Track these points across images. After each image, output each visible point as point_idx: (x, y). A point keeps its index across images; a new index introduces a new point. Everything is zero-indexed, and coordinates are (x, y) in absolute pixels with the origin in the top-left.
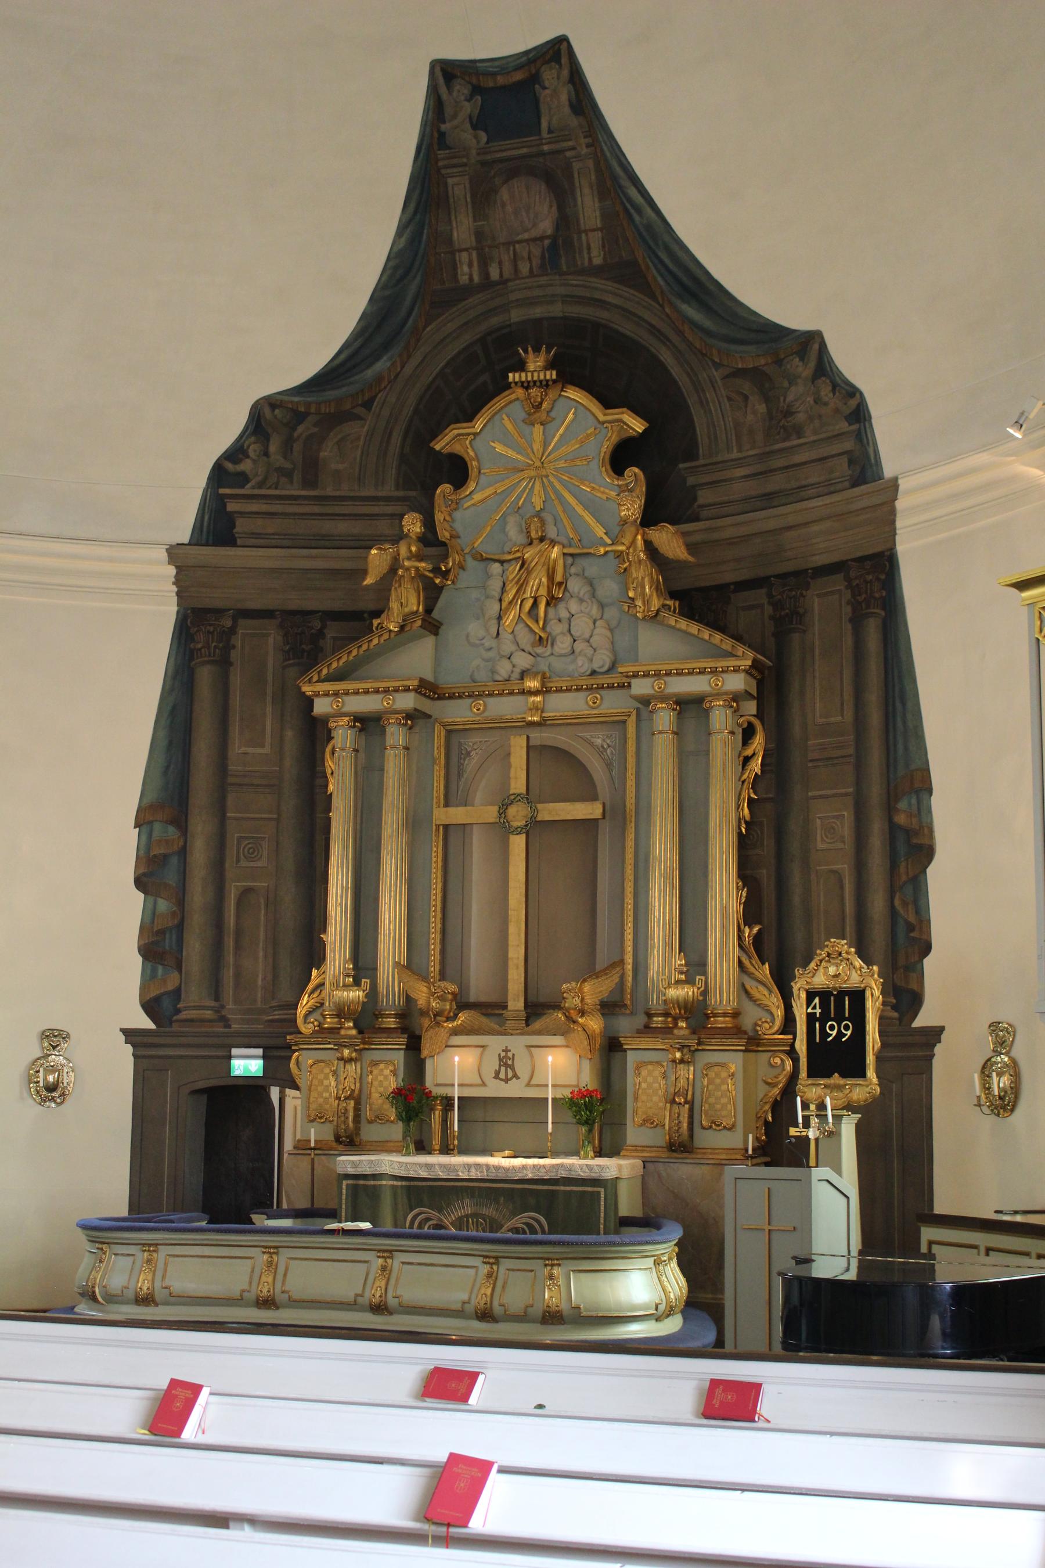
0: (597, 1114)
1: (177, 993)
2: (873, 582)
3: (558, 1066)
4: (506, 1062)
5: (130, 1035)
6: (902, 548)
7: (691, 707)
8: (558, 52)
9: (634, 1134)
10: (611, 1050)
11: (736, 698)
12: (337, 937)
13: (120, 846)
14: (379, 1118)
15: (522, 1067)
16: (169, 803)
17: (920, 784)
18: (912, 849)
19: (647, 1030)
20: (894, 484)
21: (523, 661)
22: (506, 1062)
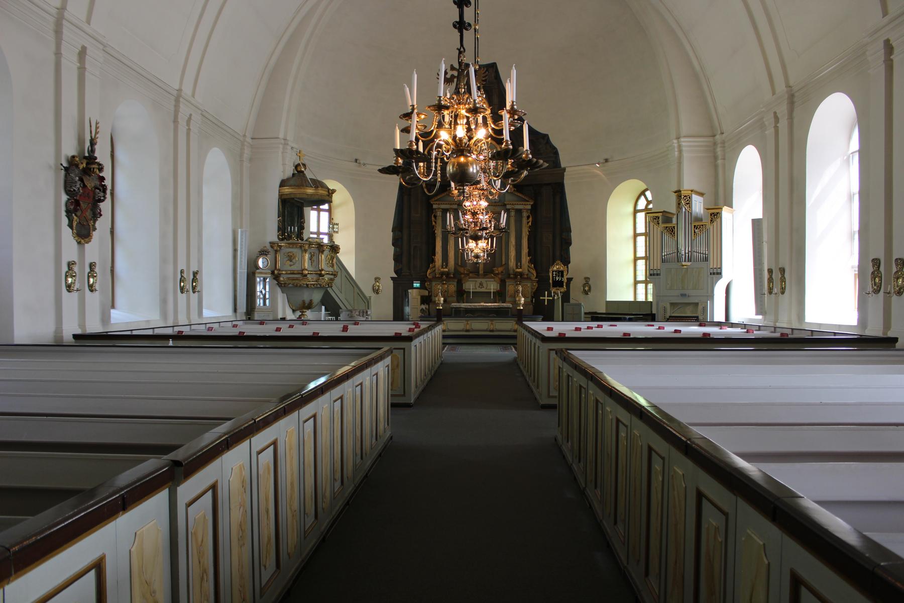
0: (500, 295)
1: (401, 269)
2: (558, 189)
3: (492, 286)
4: (481, 284)
5: (392, 278)
6: (566, 182)
7: (519, 212)
8: (495, 64)
9: (507, 299)
10: (503, 283)
12: (438, 257)
13: (389, 236)
14: (452, 296)
15: (485, 285)
16: (398, 227)
17: (569, 230)
18: (567, 243)
19: (509, 277)
20: (564, 170)
22: (481, 284)
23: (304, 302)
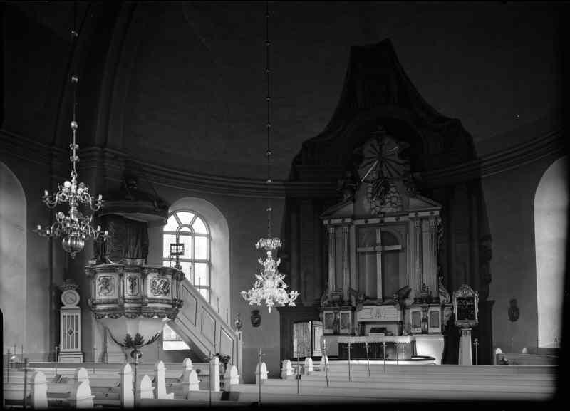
11: (436, 218)
21: (378, 209)
23: (128, 336)
